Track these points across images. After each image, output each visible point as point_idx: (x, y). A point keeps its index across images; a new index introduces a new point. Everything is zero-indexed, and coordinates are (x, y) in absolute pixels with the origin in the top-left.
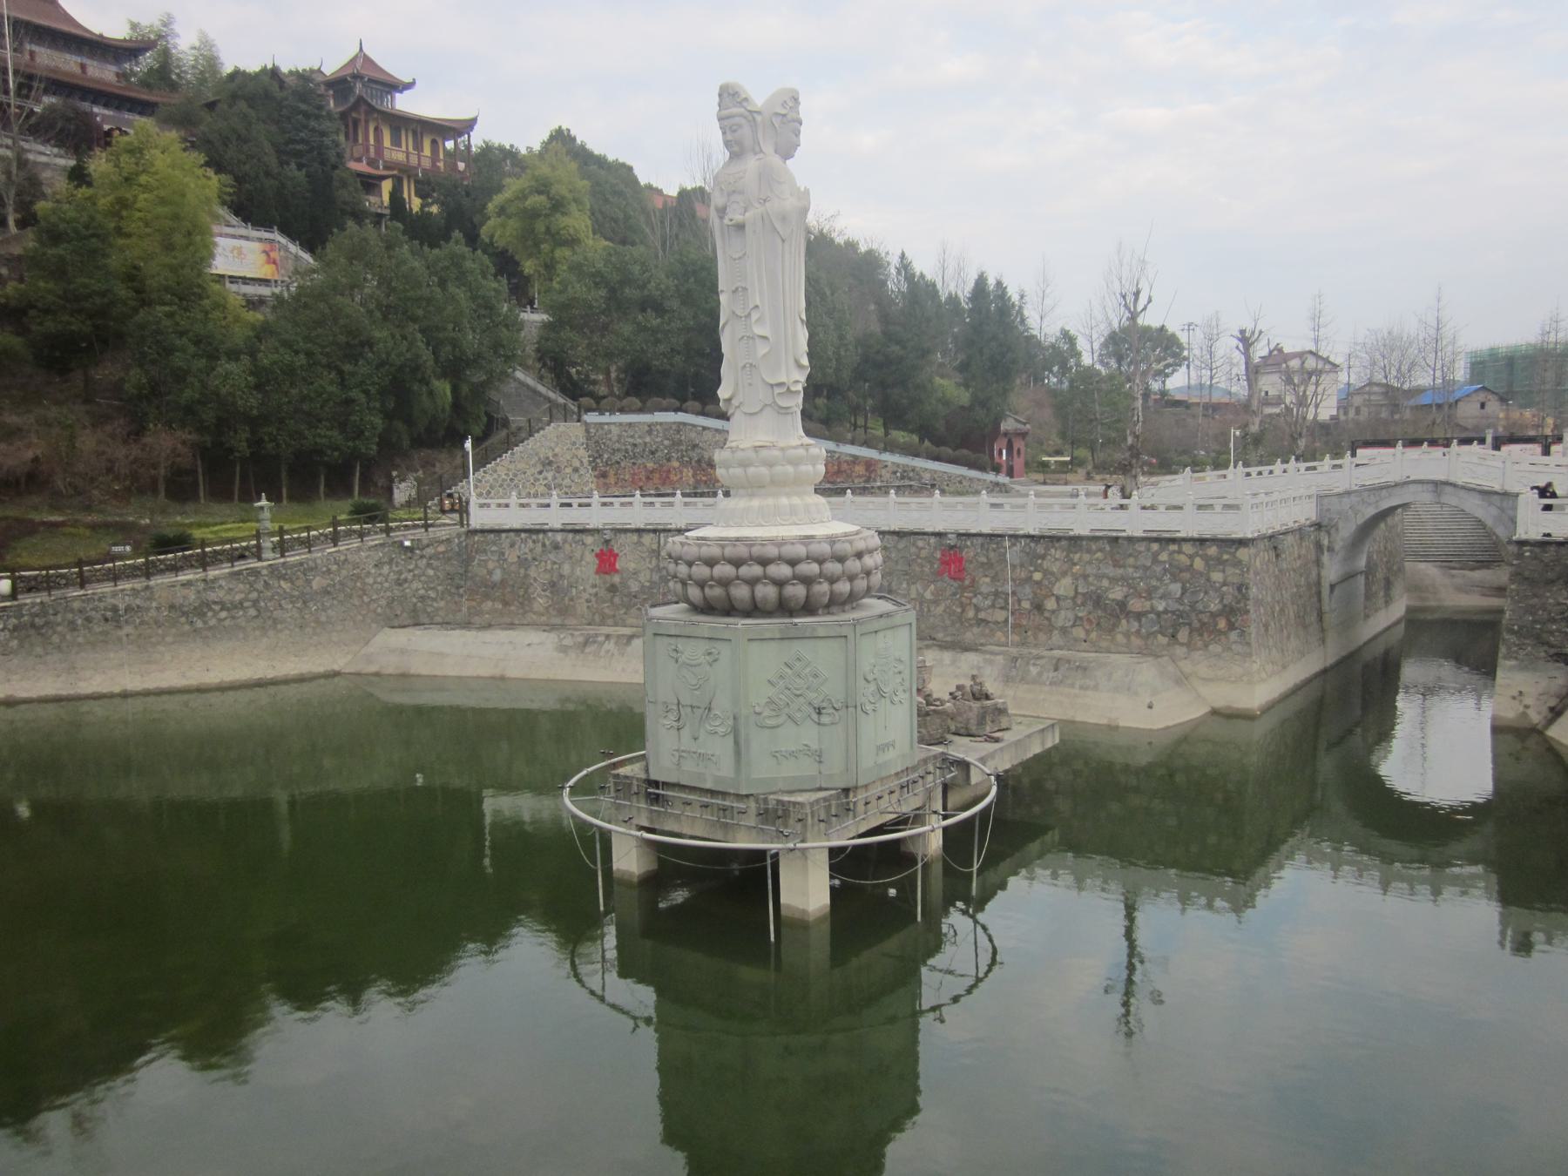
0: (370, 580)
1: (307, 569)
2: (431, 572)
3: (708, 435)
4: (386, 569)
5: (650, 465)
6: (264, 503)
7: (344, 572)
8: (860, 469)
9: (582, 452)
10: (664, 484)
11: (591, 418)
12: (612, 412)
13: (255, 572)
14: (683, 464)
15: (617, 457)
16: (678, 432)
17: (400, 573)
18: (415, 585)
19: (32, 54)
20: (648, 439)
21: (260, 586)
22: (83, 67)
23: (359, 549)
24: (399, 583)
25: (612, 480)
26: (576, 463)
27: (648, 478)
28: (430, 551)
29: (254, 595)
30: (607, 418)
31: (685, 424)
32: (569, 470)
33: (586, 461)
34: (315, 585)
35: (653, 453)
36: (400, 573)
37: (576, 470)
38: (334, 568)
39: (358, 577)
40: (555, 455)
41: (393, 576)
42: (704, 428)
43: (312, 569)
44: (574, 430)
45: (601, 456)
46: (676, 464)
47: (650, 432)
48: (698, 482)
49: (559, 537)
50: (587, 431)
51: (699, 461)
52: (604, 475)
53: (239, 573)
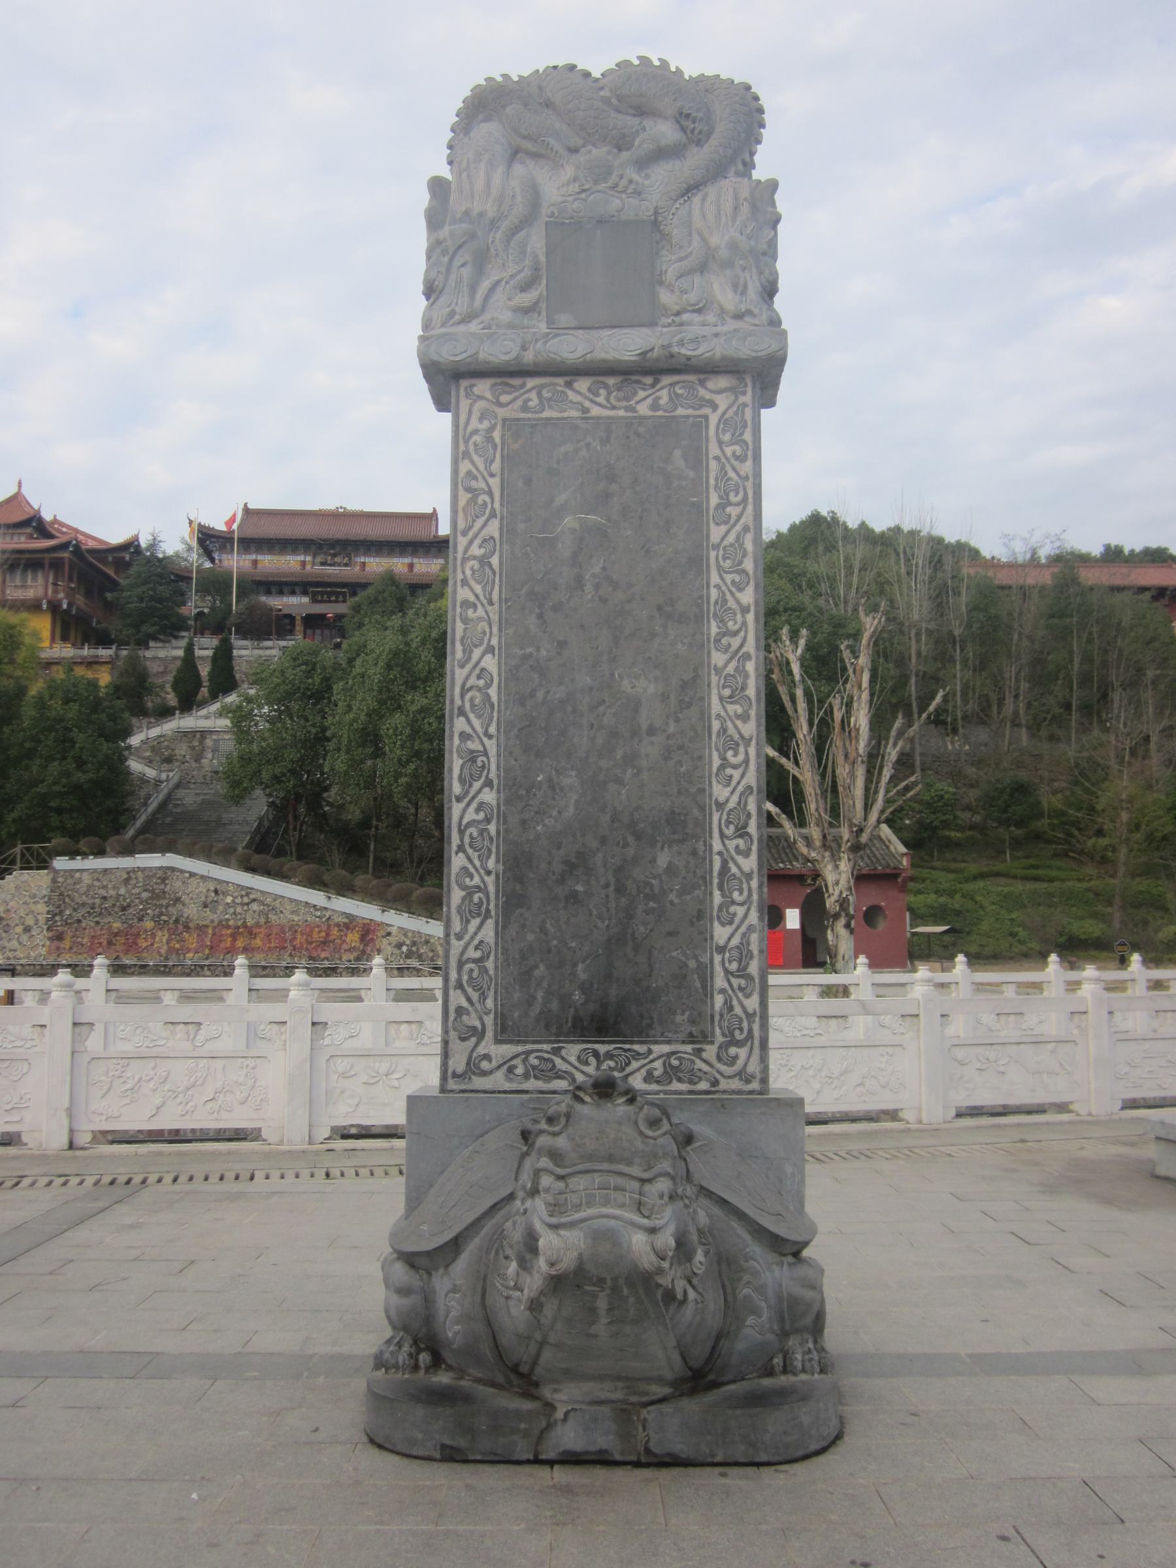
3: (194, 882)
5: (117, 925)
8: (353, 938)
9: (42, 908)
10: (127, 952)
11: (61, 863)
12: (85, 855)
14: (160, 924)
15: (82, 911)
16: (163, 880)
19: (364, 564)
20: (122, 891)
22: (411, 566)
25: (67, 944)
26: (30, 921)
27: (110, 943)
30: (78, 863)
31: (173, 869)
32: (19, 929)
33: (42, 919)
35: (124, 909)
37: (27, 929)
40: (8, 910)
42: (192, 875)
44: (37, 881)
45: (61, 913)
46: (149, 924)
47: (127, 881)
48: (171, 950)
50: (54, 881)
51: (177, 921)
52: (59, 937)
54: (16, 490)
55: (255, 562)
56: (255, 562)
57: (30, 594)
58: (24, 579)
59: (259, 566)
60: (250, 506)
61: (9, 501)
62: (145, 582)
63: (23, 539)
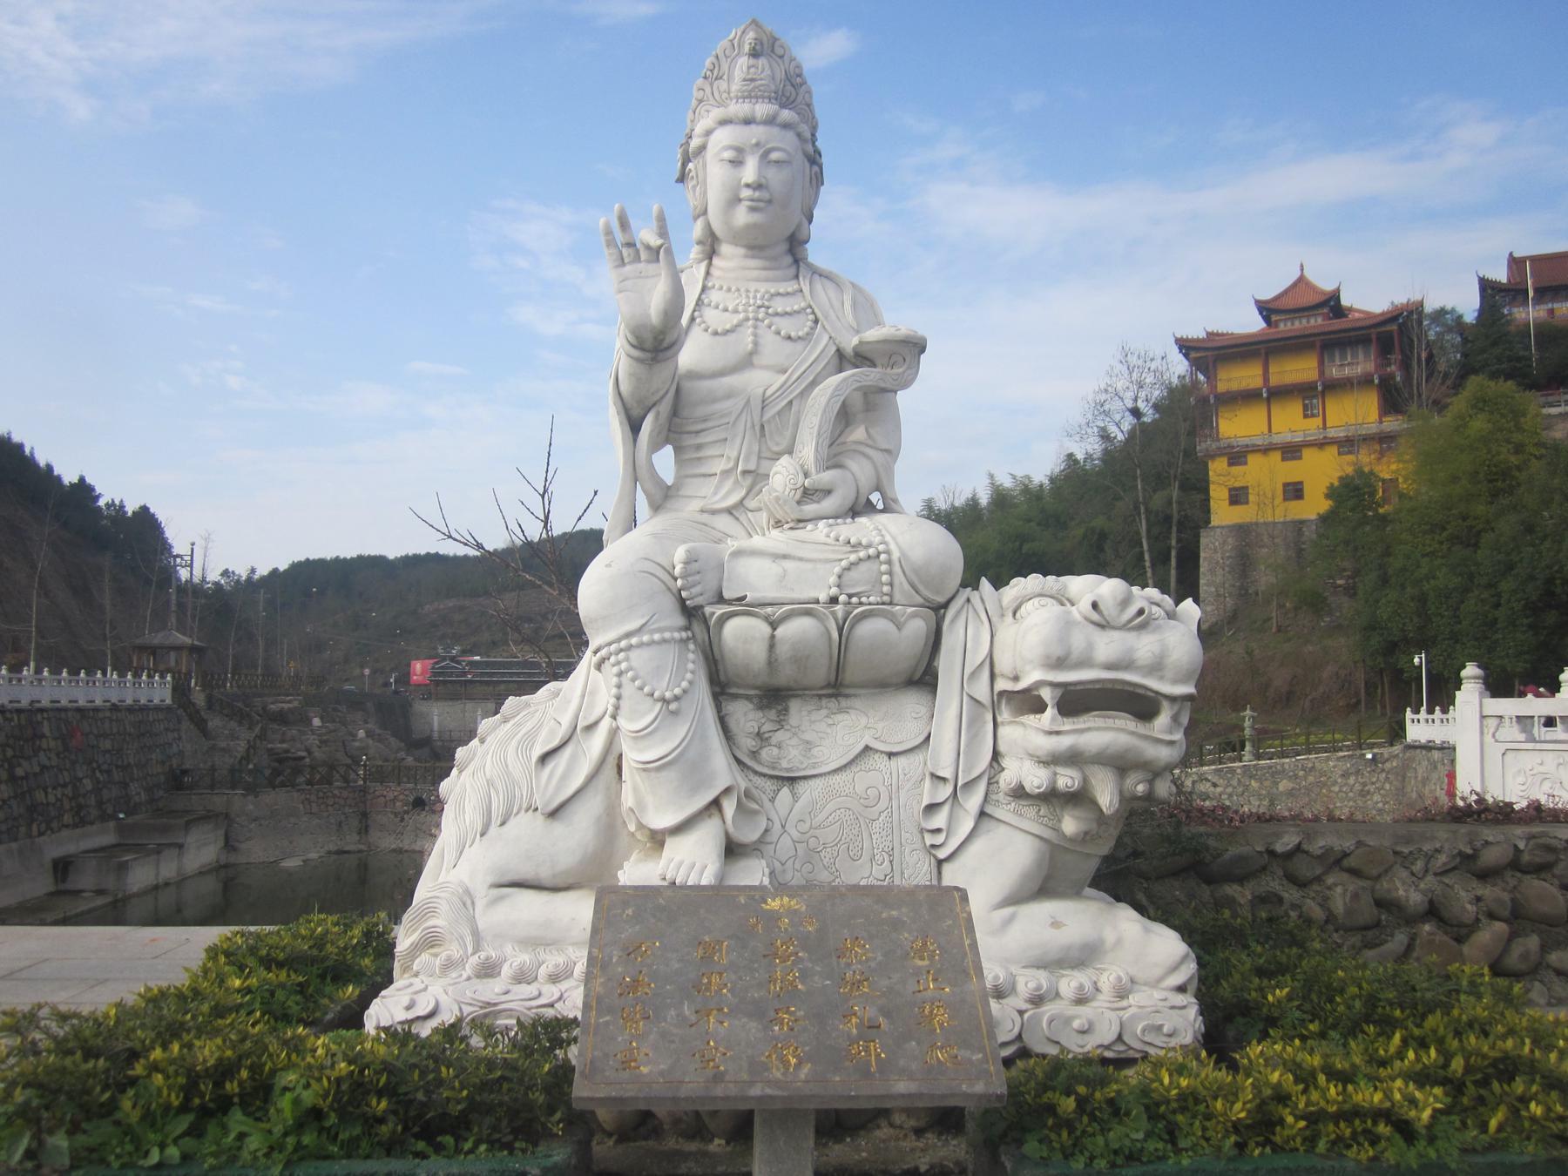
0: (1336, 789)
1: (1276, 774)
2: (1387, 786)
4: (1352, 780)
6: (1248, 712)
7: (1311, 779)
13: (1232, 771)
17: (1364, 784)
18: (1376, 798)
21: (1235, 782)
23: (1328, 759)
24: (1364, 794)
28: (1388, 765)
29: (1230, 790)
34: (1281, 787)
36: (1364, 784)
38: (1301, 773)
39: (1325, 784)
41: (1358, 787)
43: (1278, 773)
49: (1436, 755)
53: (1220, 770)
54: (1298, 274)
55: (1551, 312)
56: (1551, 312)
57: (1359, 370)
58: (1343, 357)
59: (1557, 313)
60: (1516, 255)
61: (1295, 285)
62: (1495, 344)
63: (1320, 320)
